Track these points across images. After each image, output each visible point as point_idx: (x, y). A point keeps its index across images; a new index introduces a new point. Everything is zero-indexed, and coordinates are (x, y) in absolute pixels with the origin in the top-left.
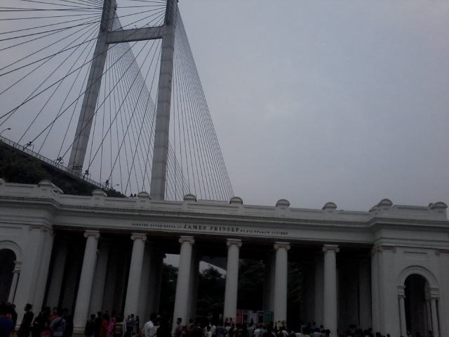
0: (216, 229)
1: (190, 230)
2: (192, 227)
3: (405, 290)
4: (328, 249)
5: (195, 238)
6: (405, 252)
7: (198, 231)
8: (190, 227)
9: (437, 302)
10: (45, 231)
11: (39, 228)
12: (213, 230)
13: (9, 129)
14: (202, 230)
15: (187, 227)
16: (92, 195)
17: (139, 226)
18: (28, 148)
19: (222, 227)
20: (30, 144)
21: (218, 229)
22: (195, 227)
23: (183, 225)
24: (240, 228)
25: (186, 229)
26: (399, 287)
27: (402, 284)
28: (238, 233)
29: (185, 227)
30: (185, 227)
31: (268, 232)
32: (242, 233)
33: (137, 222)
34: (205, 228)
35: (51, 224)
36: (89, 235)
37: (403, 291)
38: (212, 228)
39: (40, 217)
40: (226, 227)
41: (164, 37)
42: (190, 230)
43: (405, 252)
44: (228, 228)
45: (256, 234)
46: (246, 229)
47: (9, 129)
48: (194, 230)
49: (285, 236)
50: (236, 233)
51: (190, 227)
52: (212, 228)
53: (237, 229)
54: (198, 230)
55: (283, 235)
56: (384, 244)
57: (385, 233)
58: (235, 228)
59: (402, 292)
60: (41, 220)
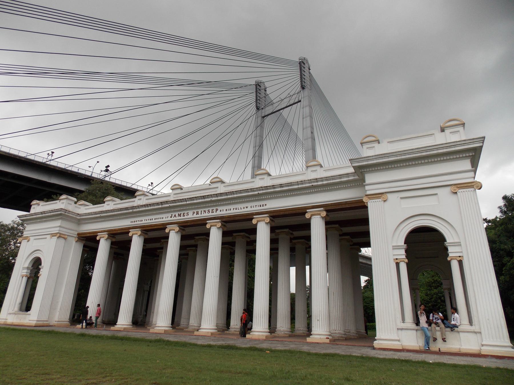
1: (175, 218)
2: (177, 215)
3: (406, 251)
4: (312, 215)
5: (179, 226)
6: (401, 198)
7: (182, 218)
8: (175, 216)
9: (460, 263)
10: (65, 239)
11: (55, 236)
12: (195, 215)
14: (186, 217)
15: (173, 216)
16: (104, 202)
17: (135, 223)
19: (203, 210)
21: (200, 213)
22: (180, 215)
23: (170, 215)
24: (220, 208)
25: (172, 218)
26: (395, 248)
27: (401, 242)
28: (219, 213)
29: (171, 217)
30: (171, 217)
31: (247, 207)
32: (222, 213)
33: (133, 220)
35: (76, 233)
36: (100, 238)
37: (403, 252)
38: (194, 213)
39: (55, 226)
40: (207, 209)
42: (175, 218)
43: (401, 198)
44: (209, 211)
45: (235, 211)
46: (225, 208)
48: (179, 218)
49: (265, 207)
50: (215, 214)
51: (175, 216)
52: (194, 213)
53: (217, 210)
54: (182, 217)
55: (262, 208)
56: (368, 193)
57: (370, 178)
58: (215, 208)
59: (401, 254)
60: (58, 229)
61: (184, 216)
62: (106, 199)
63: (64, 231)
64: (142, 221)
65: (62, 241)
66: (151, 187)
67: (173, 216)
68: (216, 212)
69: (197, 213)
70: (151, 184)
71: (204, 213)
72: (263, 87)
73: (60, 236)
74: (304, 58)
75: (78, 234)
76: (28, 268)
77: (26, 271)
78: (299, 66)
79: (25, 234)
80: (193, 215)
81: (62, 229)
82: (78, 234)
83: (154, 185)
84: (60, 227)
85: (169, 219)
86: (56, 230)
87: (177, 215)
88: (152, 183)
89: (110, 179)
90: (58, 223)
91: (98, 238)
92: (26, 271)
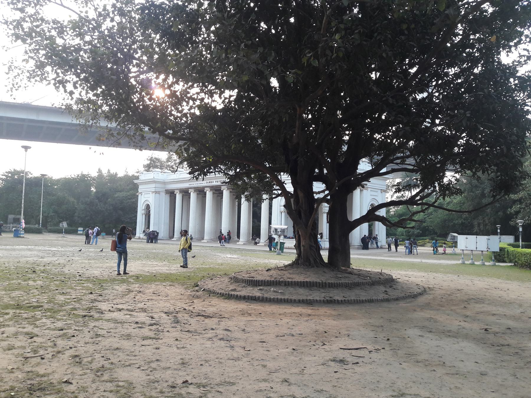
10: (159, 194)
22: (210, 182)
63: (158, 190)
65: (157, 195)
73: (156, 192)
75: (166, 190)
76: (144, 210)
77: (143, 211)
79: (140, 191)
81: (156, 189)
82: (166, 190)
84: (155, 187)
85: (206, 184)
86: (153, 190)
90: (153, 185)
92: (143, 211)
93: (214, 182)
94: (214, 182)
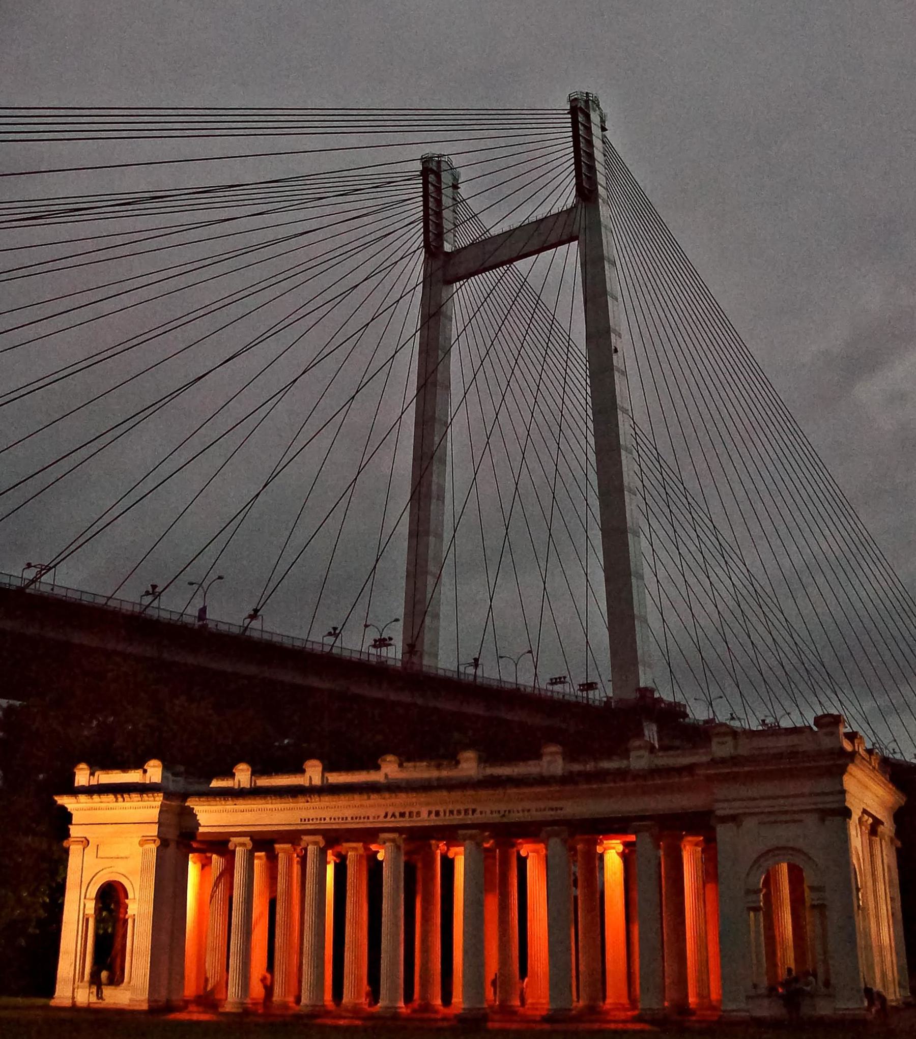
0: (437, 814)
2: (397, 814)
8: (393, 815)
13: (220, 578)
15: (390, 815)
18: (256, 624)
20: (254, 616)
21: (442, 814)
22: (402, 815)
29: (386, 816)
34: (418, 814)
41: (581, 237)
47: (220, 578)
48: (401, 819)
52: (430, 813)
53: (474, 811)
61: (412, 817)
62: (239, 768)
64: (325, 819)
66: (148, 599)
67: (390, 815)
68: (473, 814)
69: (437, 814)
70: (151, 591)
71: (451, 815)
72: (446, 178)
74: (587, 93)
78: (570, 116)
80: (429, 816)
83: (158, 590)
87: (397, 814)
88: (154, 587)
89: (52, 589)
91: (231, 846)
93: (424, 815)
94: (424, 815)
